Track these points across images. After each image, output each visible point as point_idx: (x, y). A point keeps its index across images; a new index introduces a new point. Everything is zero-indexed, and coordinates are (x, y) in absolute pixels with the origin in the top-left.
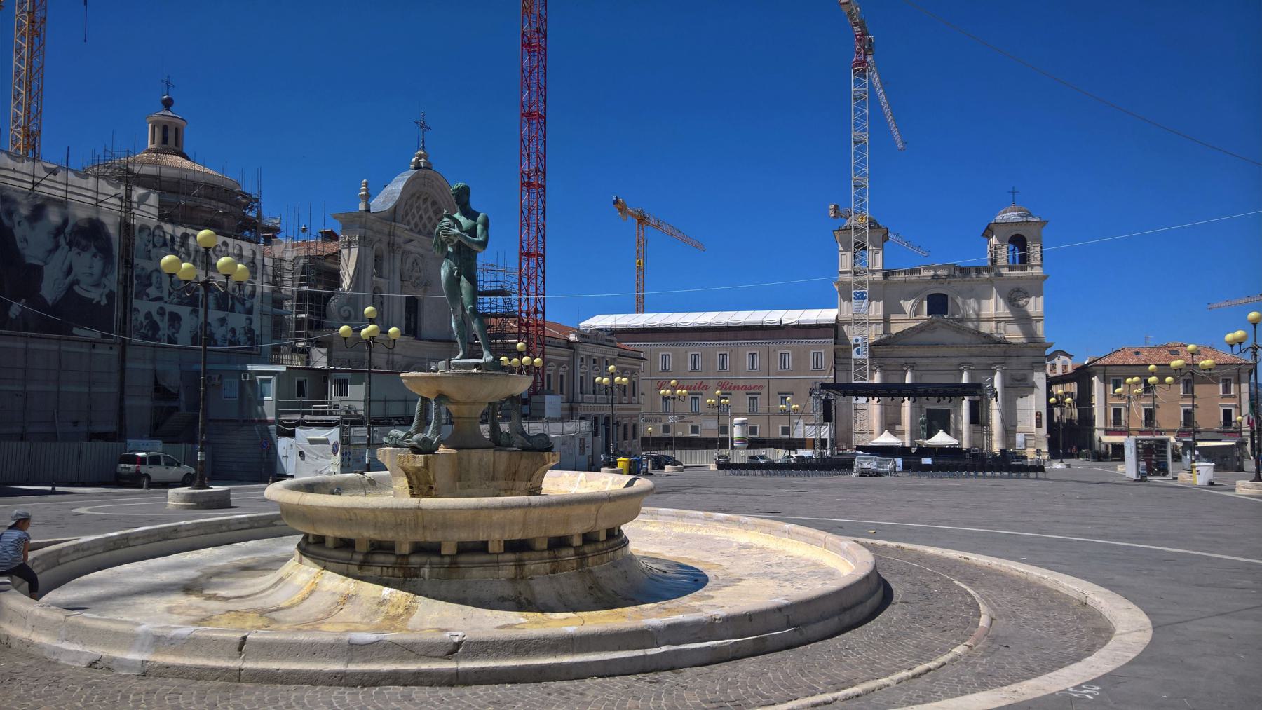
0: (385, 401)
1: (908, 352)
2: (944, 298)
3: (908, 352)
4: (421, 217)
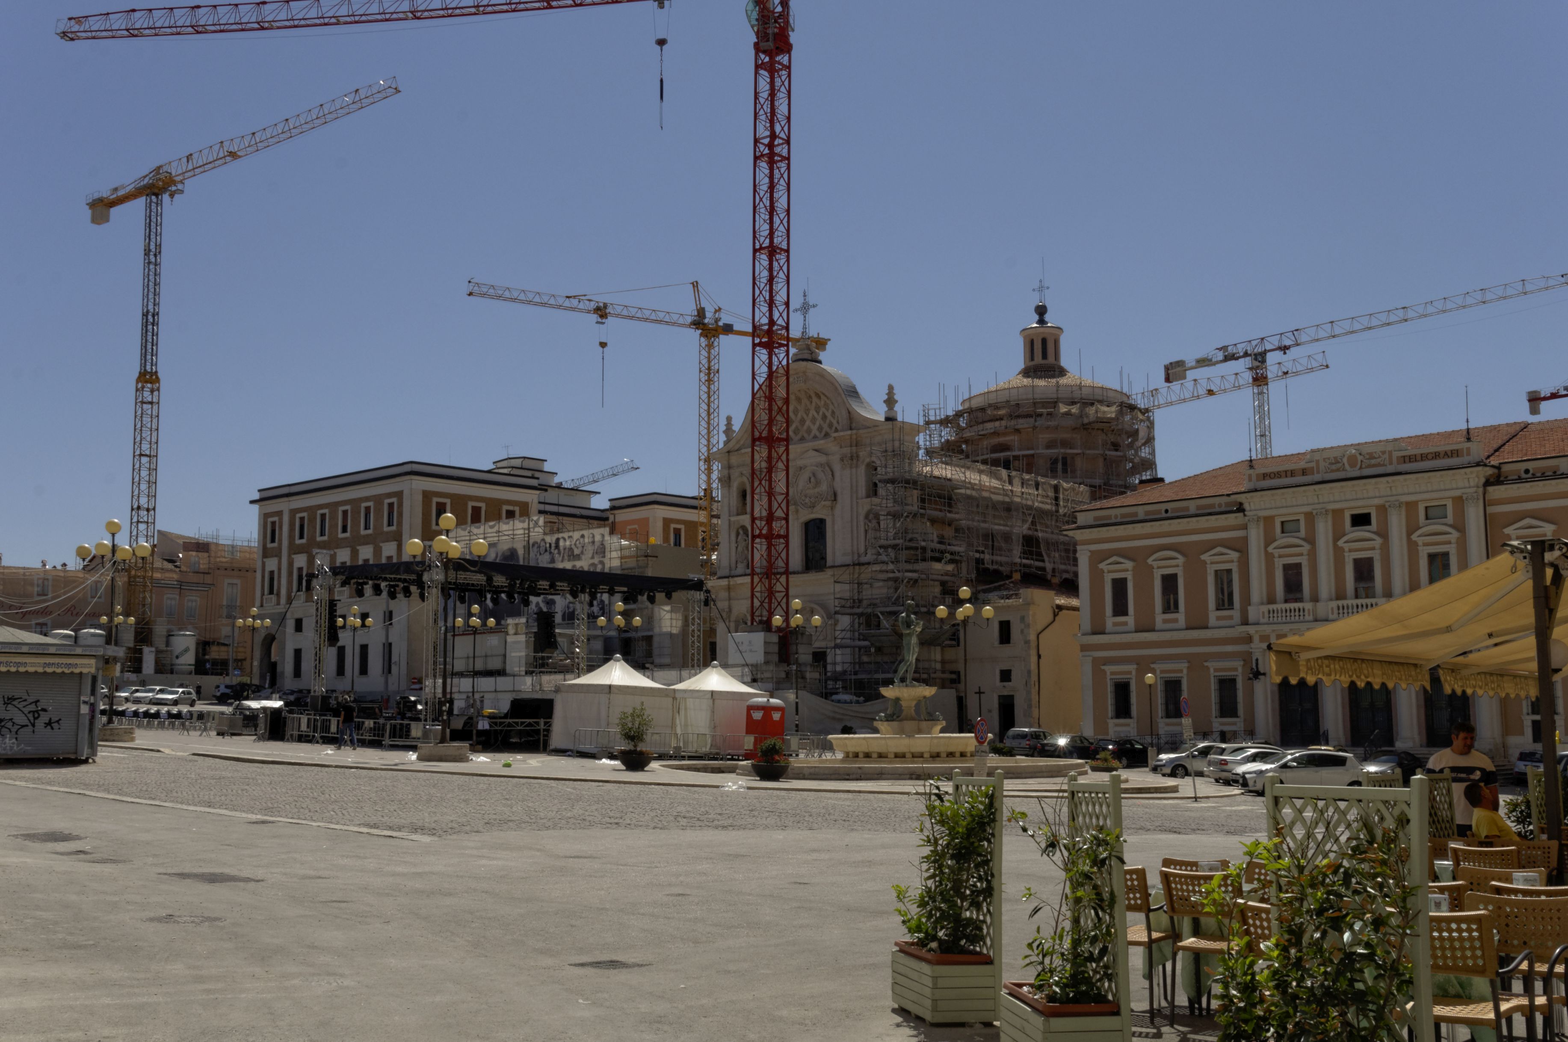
0: (486, 656)
4: (824, 417)
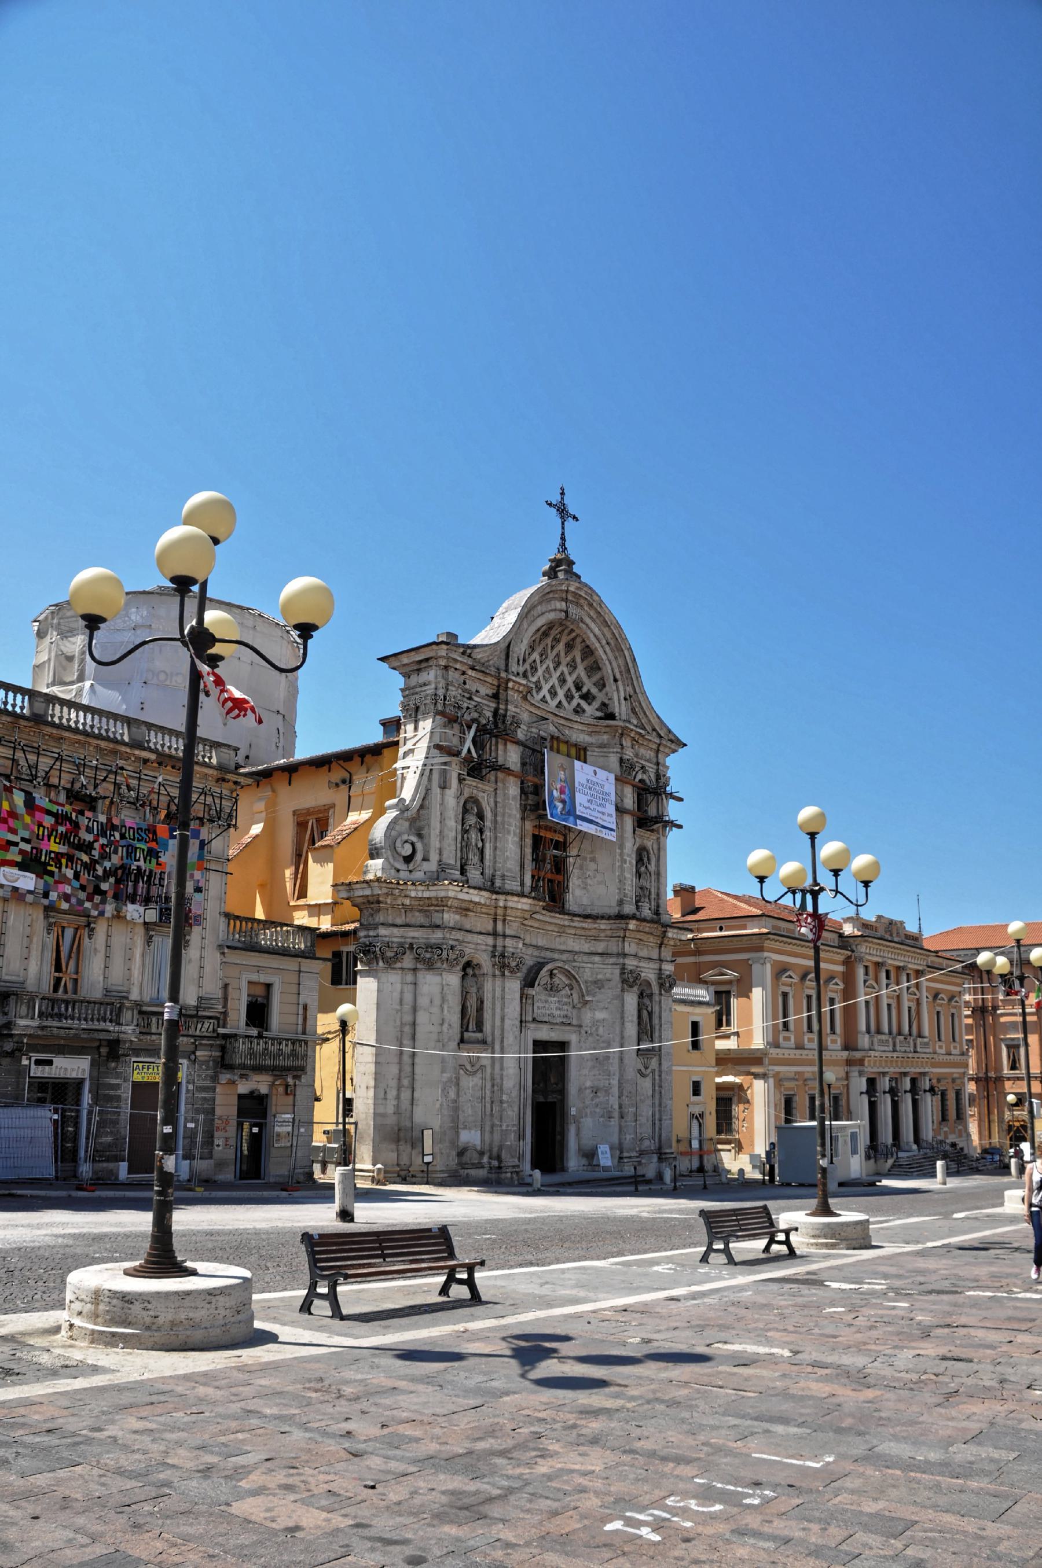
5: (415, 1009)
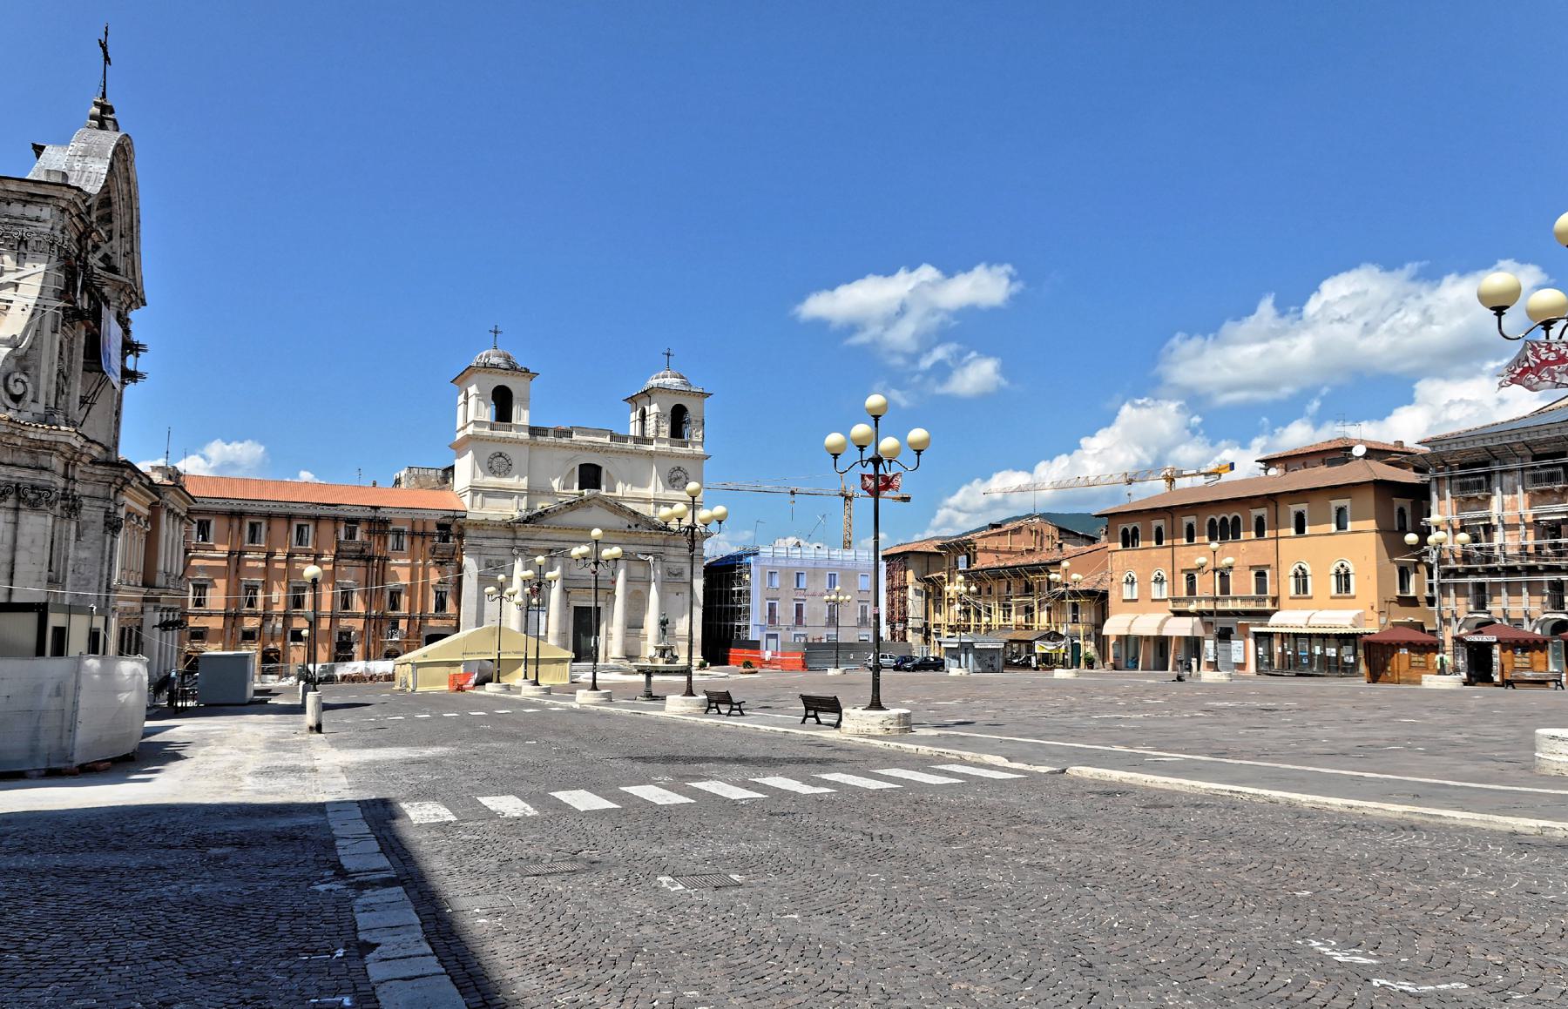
1: (556, 536)
2: (598, 469)
3: (556, 536)
5: (14, 549)
